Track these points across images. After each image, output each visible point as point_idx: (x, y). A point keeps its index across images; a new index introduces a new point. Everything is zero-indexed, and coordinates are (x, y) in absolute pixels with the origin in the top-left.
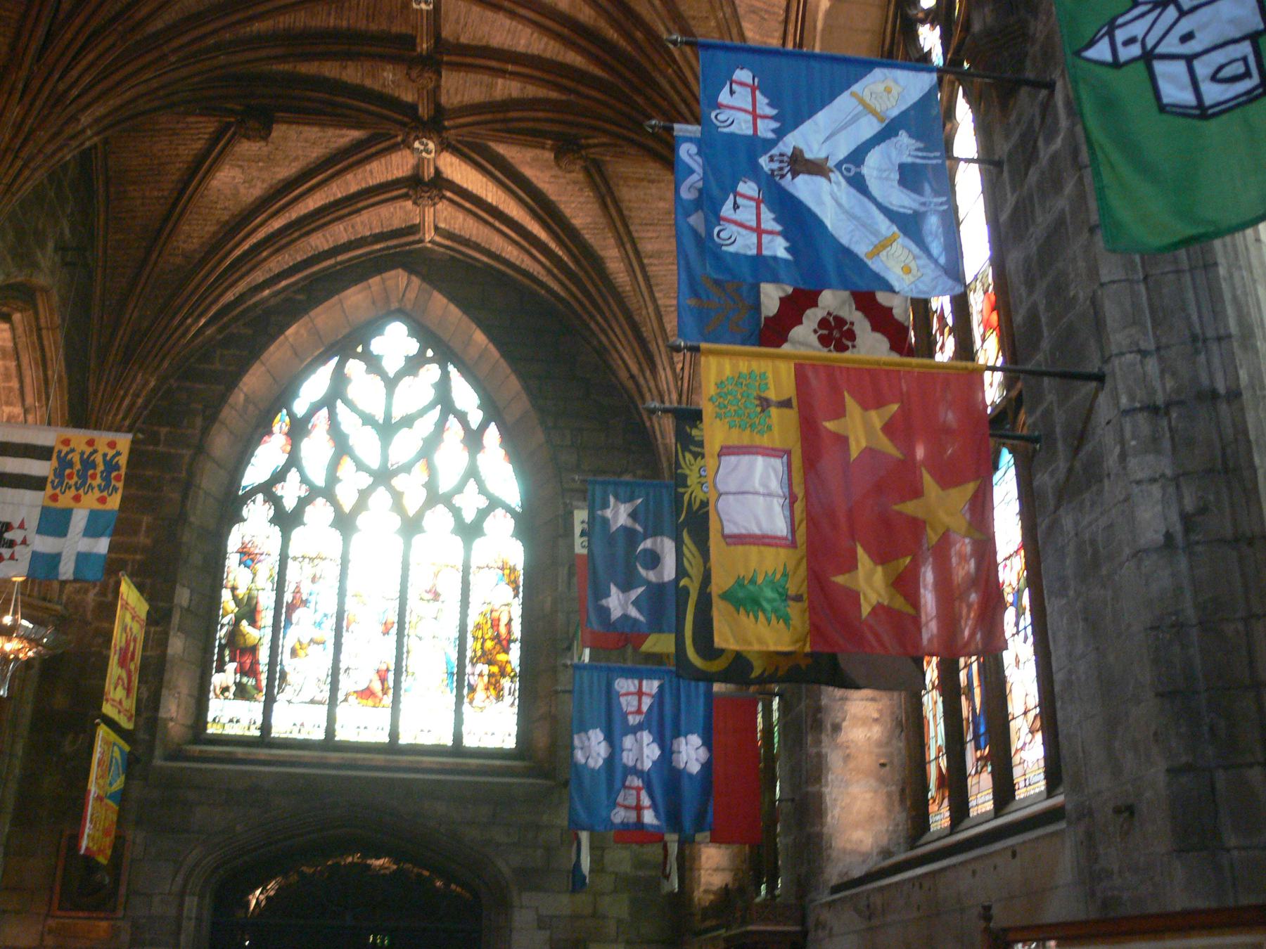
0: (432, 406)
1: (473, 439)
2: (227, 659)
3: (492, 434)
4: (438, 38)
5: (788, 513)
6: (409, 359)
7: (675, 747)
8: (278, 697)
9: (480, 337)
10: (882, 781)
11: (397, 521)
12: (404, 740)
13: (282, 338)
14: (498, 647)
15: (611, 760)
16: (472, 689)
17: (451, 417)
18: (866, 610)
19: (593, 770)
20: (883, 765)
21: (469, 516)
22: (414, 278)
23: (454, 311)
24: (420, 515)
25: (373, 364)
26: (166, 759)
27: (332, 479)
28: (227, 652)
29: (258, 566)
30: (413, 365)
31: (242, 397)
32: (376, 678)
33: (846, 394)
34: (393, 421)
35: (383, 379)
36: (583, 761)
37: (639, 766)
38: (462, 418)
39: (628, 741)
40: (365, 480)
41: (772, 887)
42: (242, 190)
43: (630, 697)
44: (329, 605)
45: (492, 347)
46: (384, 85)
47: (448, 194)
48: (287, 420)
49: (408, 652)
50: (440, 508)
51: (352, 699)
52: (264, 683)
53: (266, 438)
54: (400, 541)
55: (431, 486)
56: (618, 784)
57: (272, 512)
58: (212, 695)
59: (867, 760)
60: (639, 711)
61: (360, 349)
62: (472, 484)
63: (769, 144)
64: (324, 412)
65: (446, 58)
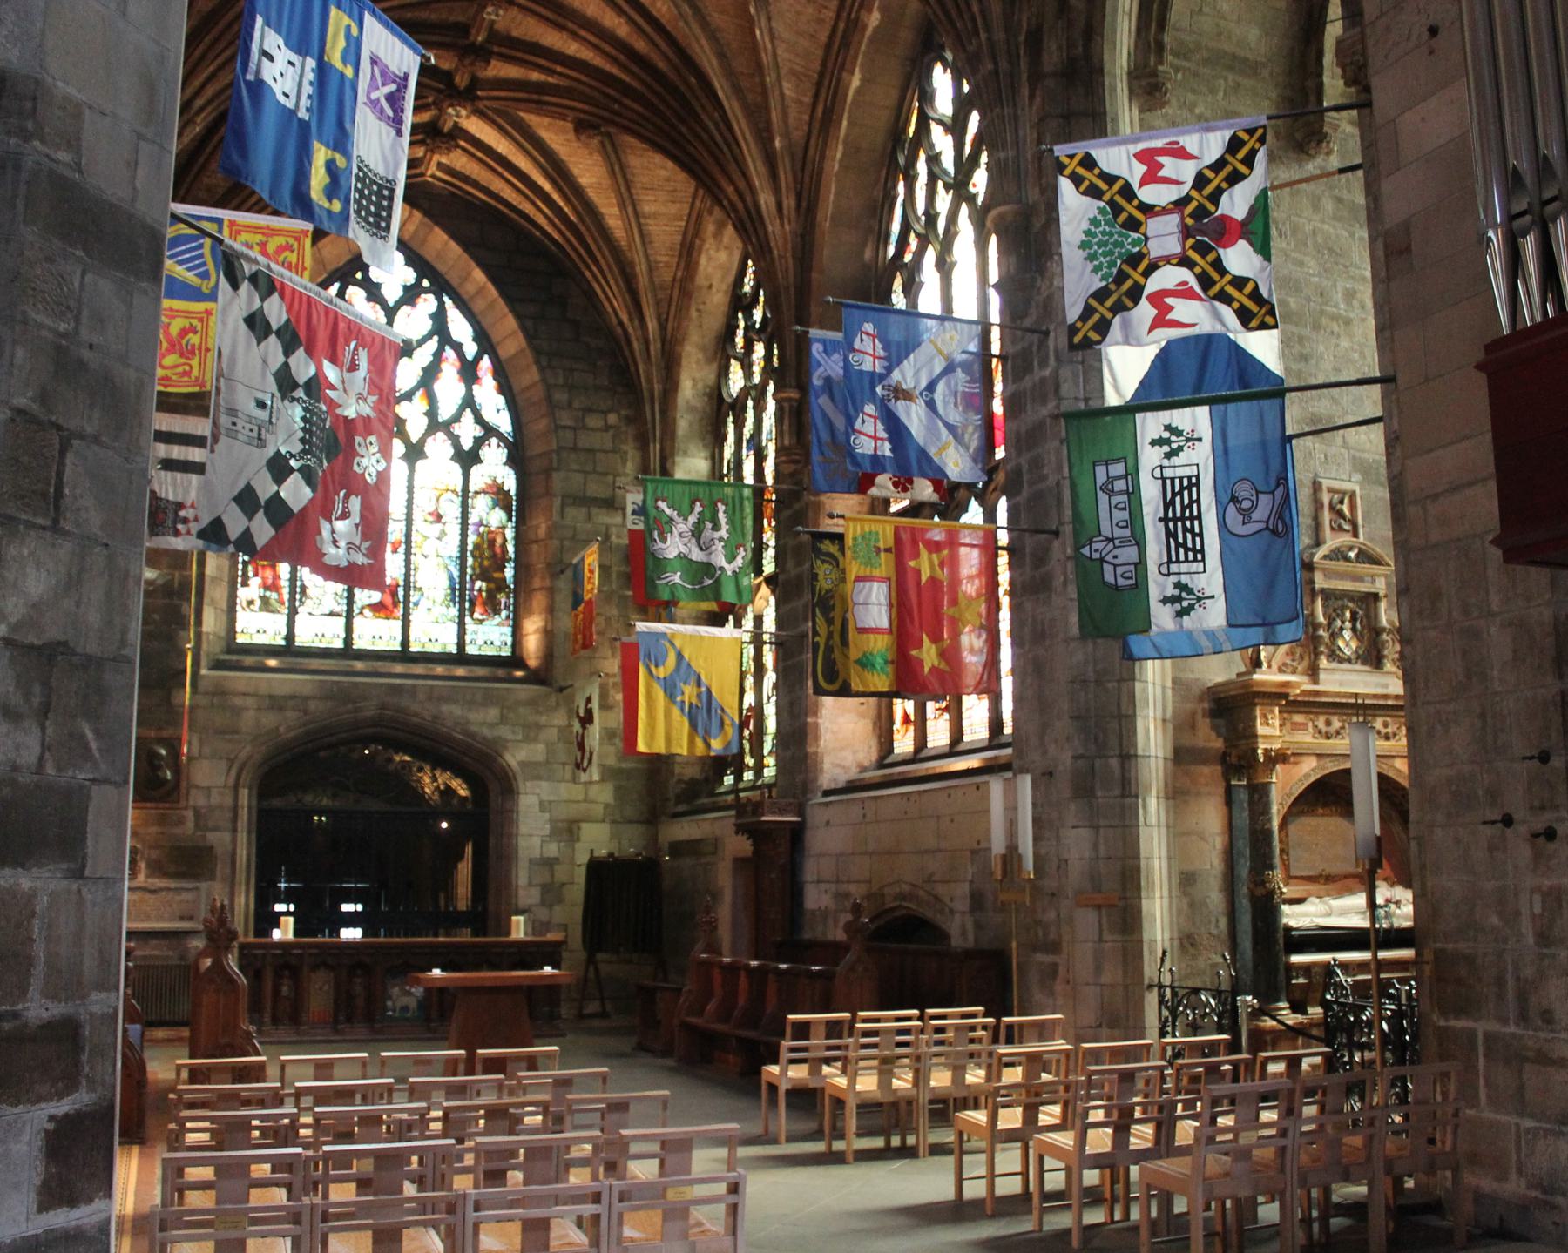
2: (251, 574)
3: (486, 363)
6: (406, 288)
9: (479, 275)
16: (473, 604)
17: (447, 348)
18: (926, 669)
21: (467, 444)
23: (455, 248)
24: (422, 441)
25: (373, 292)
26: (211, 668)
28: (250, 568)
30: (411, 295)
38: (458, 348)
41: (739, 778)
45: (490, 286)
47: (462, 143)
50: (440, 435)
51: (367, 612)
52: (286, 597)
55: (432, 414)
58: (238, 608)
61: (359, 275)
62: (468, 415)
63: (882, 377)
65: (496, 49)
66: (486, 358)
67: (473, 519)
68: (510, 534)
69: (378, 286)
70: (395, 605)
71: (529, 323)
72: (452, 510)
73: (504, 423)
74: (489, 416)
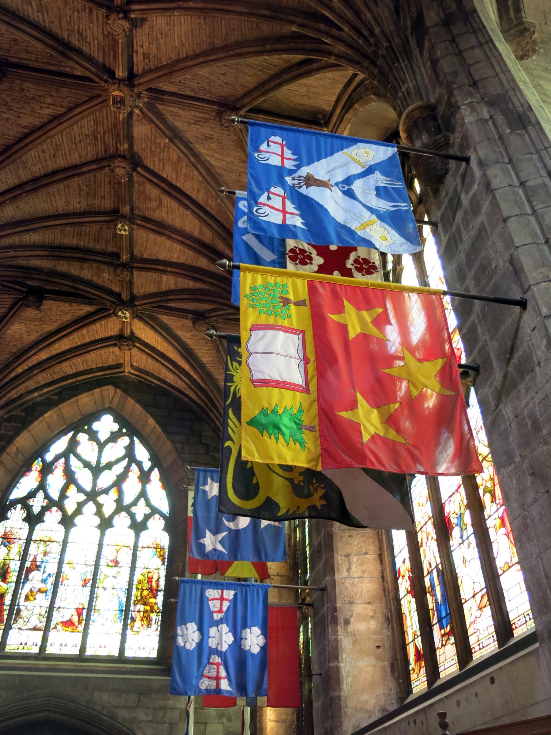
0: (122, 458)
1: (145, 477)
3: (155, 474)
4: (132, 255)
5: (302, 370)
6: (112, 433)
7: (243, 636)
8: (14, 626)
9: (151, 421)
10: (378, 658)
11: (97, 521)
12: (89, 652)
13: (42, 418)
14: (151, 594)
15: (200, 645)
16: (133, 620)
17: (133, 464)
19: (189, 650)
20: (378, 647)
21: (139, 518)
22: (118, 390)
23: (138, 407)
24: (112, 517)
25: (93, 436)
27: (63, 495)
29: (12, 546)
30: (114, 437)
31: (15, 448)
32: (75, 613)
33: (345, 300)
34: (101, 466)
35: (97, 444)
36: (182, 645)
37: (219, 649)
38: (139, 465)
39: (213, 631)
40: (82, 497)
42: (25, 336)
43: (215, 601)
44: (52, 568)
45: (157, 426)
46: (104, 282)
47: (137, 345)
48: (41, 464)
49: (97, 597)
50: (123, 514)
51: (59, 627)
53: (27, 473)
54: (98, 532)
55: (119, 501)
56: (205, 660)
57: (25, 515)
59: (369, 645)
60: (220, 611)
62: (142, 501)
64: (62, 460)
65: (135, 265)
66: (156, 469)
67: (139, 564)
68: (163, 573)
69: (96, 432)
70: (80, 623)
71: (178, 445)
72: (125, 559)
73: (164, 505)
74: (154, 502)
